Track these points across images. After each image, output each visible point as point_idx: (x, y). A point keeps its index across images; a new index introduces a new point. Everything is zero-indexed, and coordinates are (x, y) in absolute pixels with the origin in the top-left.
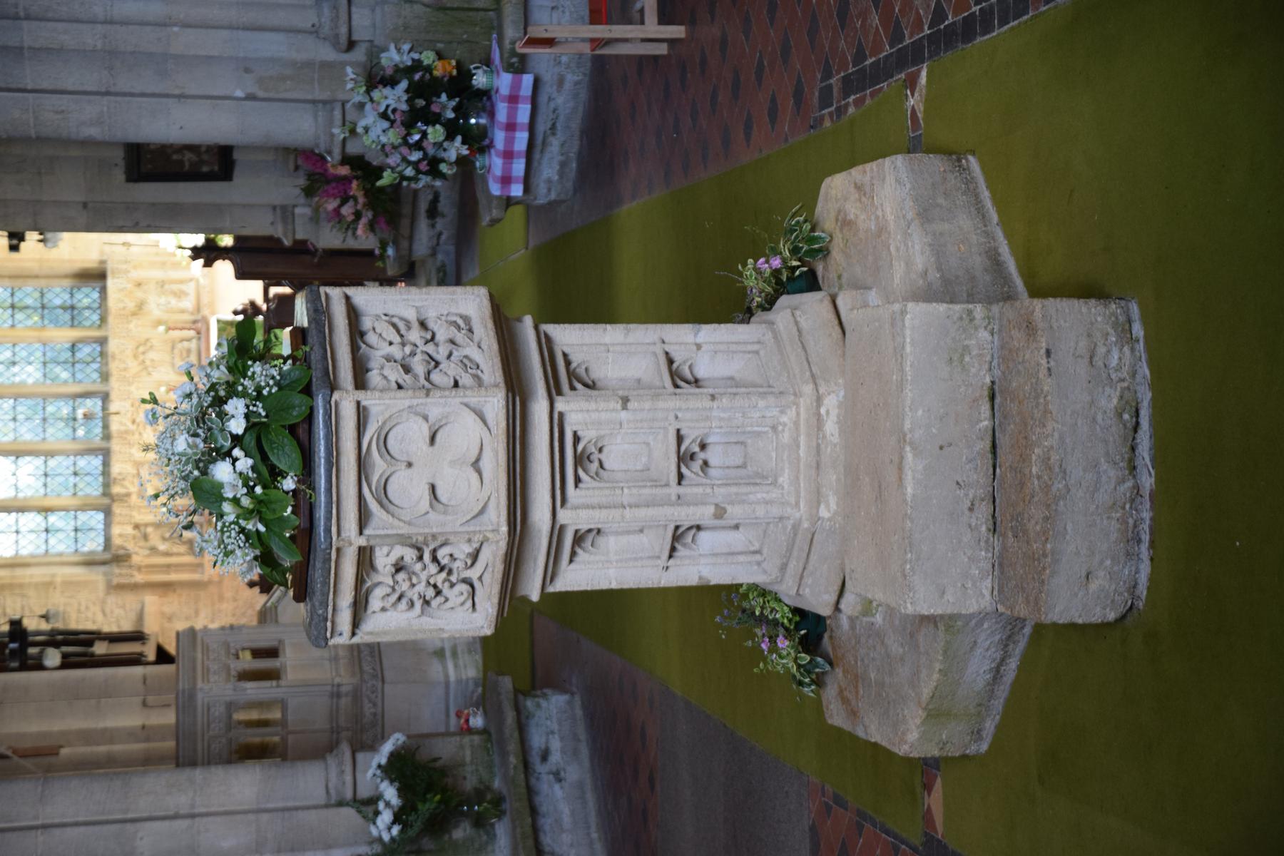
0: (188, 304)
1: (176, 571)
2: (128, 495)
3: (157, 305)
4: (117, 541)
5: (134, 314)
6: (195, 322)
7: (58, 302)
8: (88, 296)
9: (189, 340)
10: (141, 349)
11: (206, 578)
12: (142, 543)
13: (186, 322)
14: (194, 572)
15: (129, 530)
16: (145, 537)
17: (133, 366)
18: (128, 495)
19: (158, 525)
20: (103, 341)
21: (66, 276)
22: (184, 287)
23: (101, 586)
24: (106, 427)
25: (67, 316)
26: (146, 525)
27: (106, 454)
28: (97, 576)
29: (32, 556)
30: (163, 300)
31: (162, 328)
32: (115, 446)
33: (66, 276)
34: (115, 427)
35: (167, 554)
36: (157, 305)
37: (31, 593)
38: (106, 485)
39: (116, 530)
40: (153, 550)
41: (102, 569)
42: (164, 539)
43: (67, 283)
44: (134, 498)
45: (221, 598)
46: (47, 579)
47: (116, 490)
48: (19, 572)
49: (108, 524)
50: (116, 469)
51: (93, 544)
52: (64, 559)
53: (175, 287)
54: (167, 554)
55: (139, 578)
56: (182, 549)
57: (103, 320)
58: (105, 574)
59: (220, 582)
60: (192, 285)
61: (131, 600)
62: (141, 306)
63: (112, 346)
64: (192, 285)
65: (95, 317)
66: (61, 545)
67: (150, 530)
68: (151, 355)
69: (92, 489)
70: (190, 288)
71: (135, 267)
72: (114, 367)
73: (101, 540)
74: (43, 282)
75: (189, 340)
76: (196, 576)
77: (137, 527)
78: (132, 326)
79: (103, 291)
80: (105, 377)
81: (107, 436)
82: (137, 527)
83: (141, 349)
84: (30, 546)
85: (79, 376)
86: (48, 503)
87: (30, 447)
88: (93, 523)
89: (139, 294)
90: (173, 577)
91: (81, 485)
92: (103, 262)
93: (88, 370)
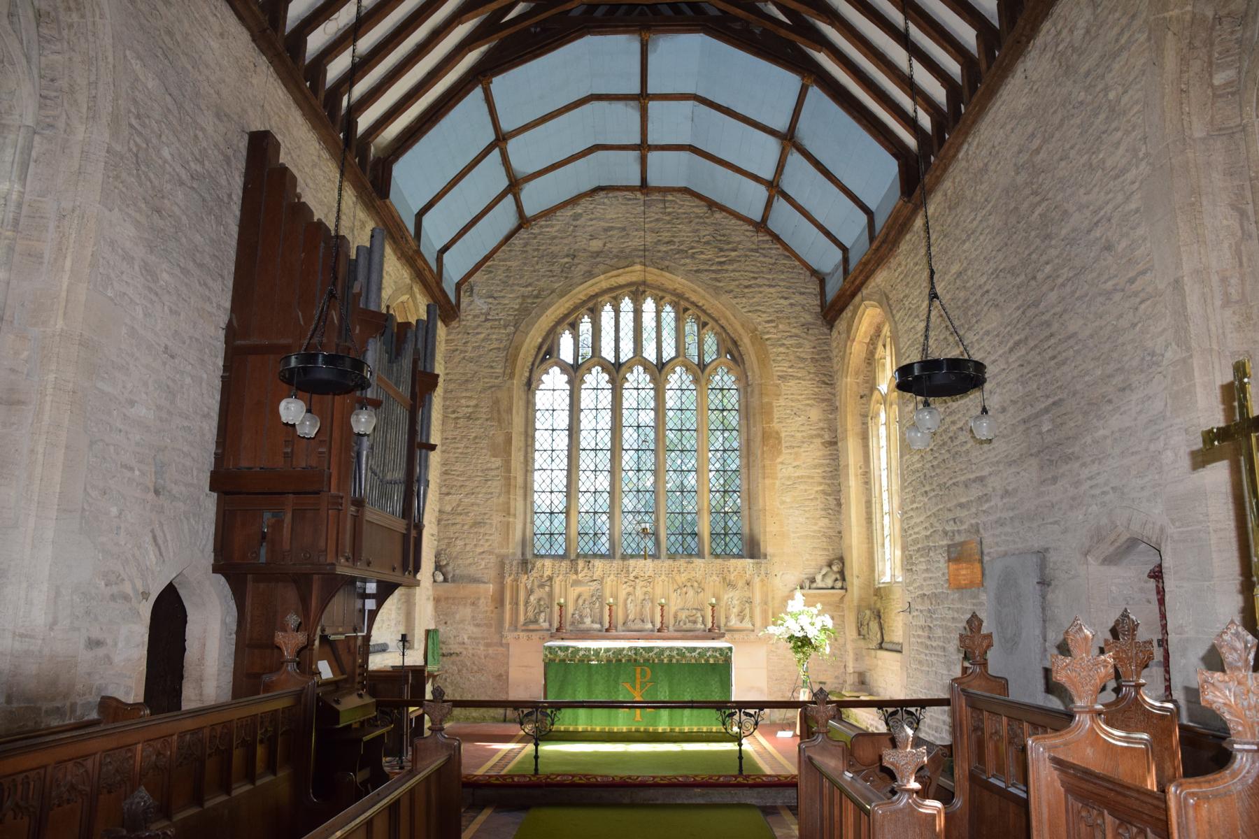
0: (734, 622)
1: (512, 609)
2: (576, 573)
3: (732, 598)
4: (539, 563)
5: (724, 579)
6: (719, 627)
7: (730, 524)
8: (735, 545)
9: (703, 622)
10: (696, 584)
11: (505, 634)
12: (536, 583)
13: (719, 620)
14: (511, 624)
15: (548, 573)
16: (542, 586)
17: (682, 578)
18: (576, 573)
19: (551, 595)
20: (700, 555)
21: (751, 529)
22: (747, 618)
23: (504, 551)
24: (632, 556)
25: (718, 530)
26: (551, 586)
27: (610, 556)
28: (513, 549)
29: (533, 502)
30: (736, 602)
31: (714, 601)
32: (617, 563)
33: (751, 529)
34: (632, 562)
35: (527, 603)
36: (732, 598)
37: (502, 499)
38: (585, 556)
39: (548, 562)
40: (531, 592)
41: (519, 553)
42: (540, 600)
43: (746, 530)
44: (574, 577)
45: (488, 645)
46: (512, 511)
47: (581, 563)
48: (520, 492)
49: (554, 557)
50: (598, 563)
51: (541, 545)
52: (528, 525)
53: (747, 611)
54: (527, 603)
55: (508, 580)
56: (531, 615)
57: (717, 556)
58: (514, 554)
59: (501, 645)
60: (750, 626)
61: (492, 573)
62: (731, 585)
63: (698, 561)
64: (750, 626)
65: (719, 551)
66: (542, 523)
67: (547, 589)
68: (691, 593)
69: (585, 546)
70: (747, 624)
71: (762, 581)
72: (682, 563)
73: (543, 552)
74: (746, 513)
75: (703, 622)
76: (507, 625)
77: (550, 579)
78: (714, 577)
79: (740, 556)
80: (672, 556)
81: (624, 557)
82: (550, 579)
83: (696, 584)
84: (541, 501)
85: (673, 538)
86: (573, 513)
87: (617, 501)
88: (556, 546)
89: (741, 583)
90: (508, 607)
91: (586, 538)
92: (765, 556)
93: (677, 545)
